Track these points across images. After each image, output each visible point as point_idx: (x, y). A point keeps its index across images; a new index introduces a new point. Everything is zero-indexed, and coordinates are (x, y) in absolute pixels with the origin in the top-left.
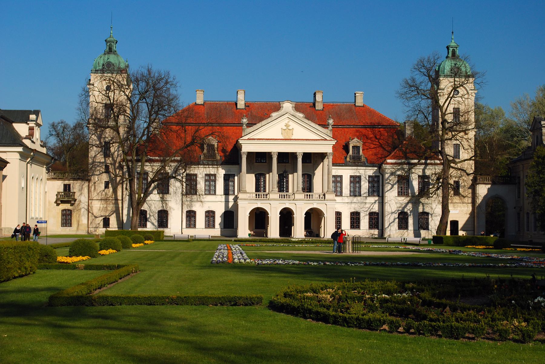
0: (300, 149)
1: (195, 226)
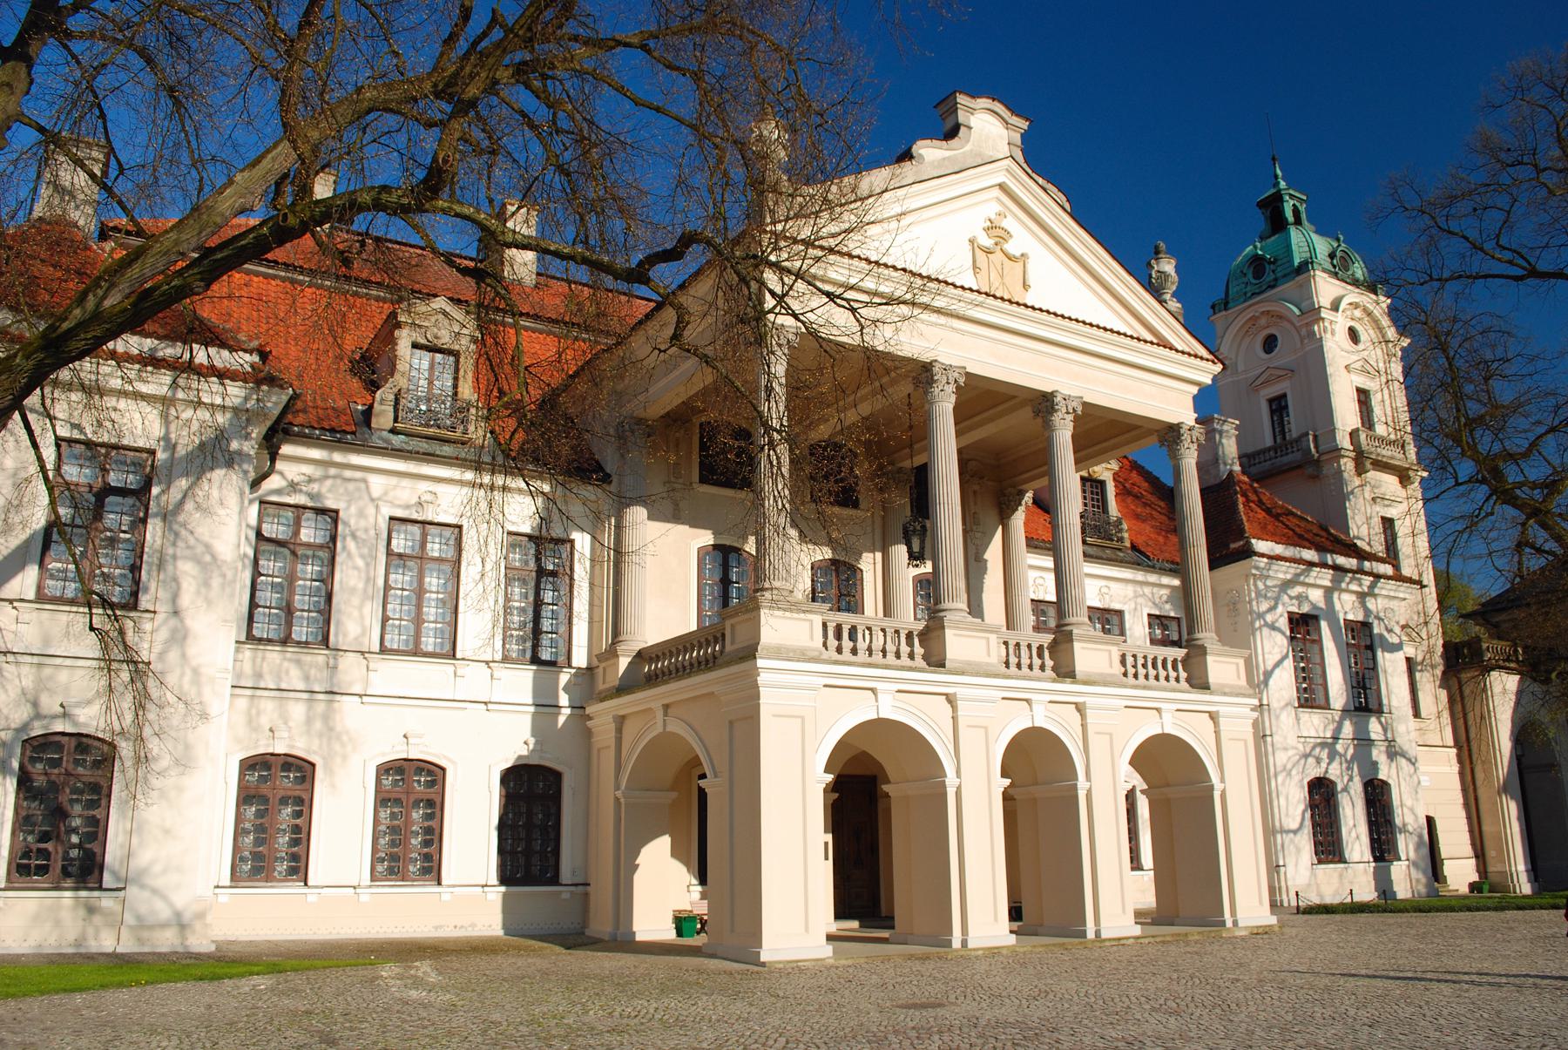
1: (298, 868)
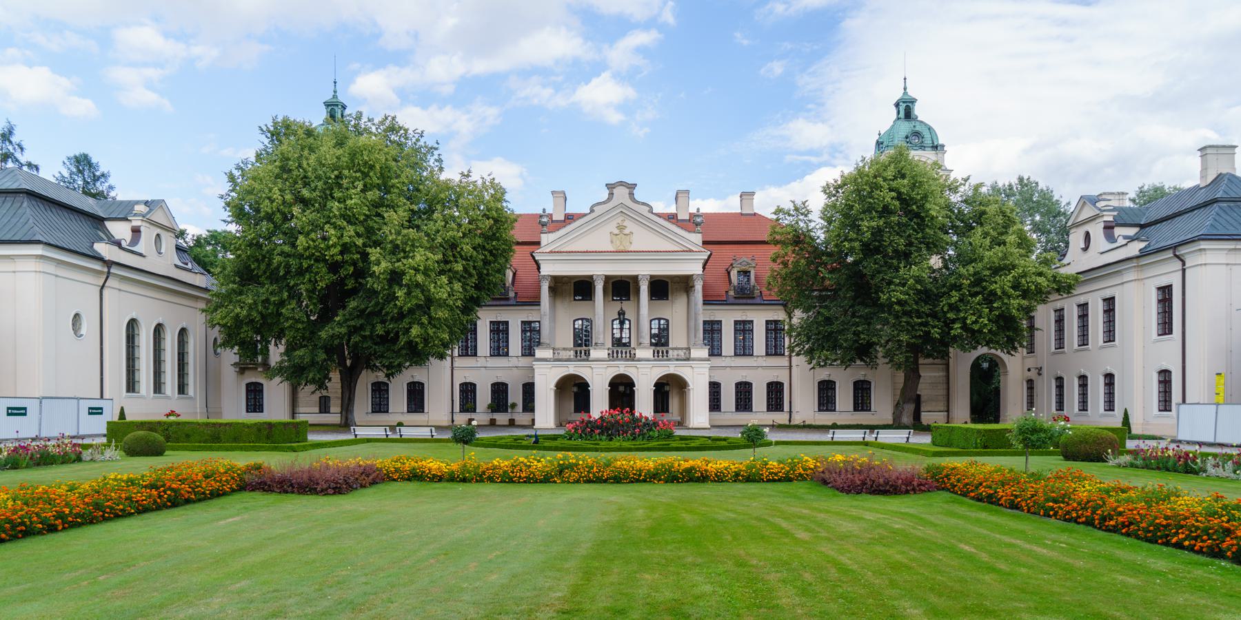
0: (645, 270)
